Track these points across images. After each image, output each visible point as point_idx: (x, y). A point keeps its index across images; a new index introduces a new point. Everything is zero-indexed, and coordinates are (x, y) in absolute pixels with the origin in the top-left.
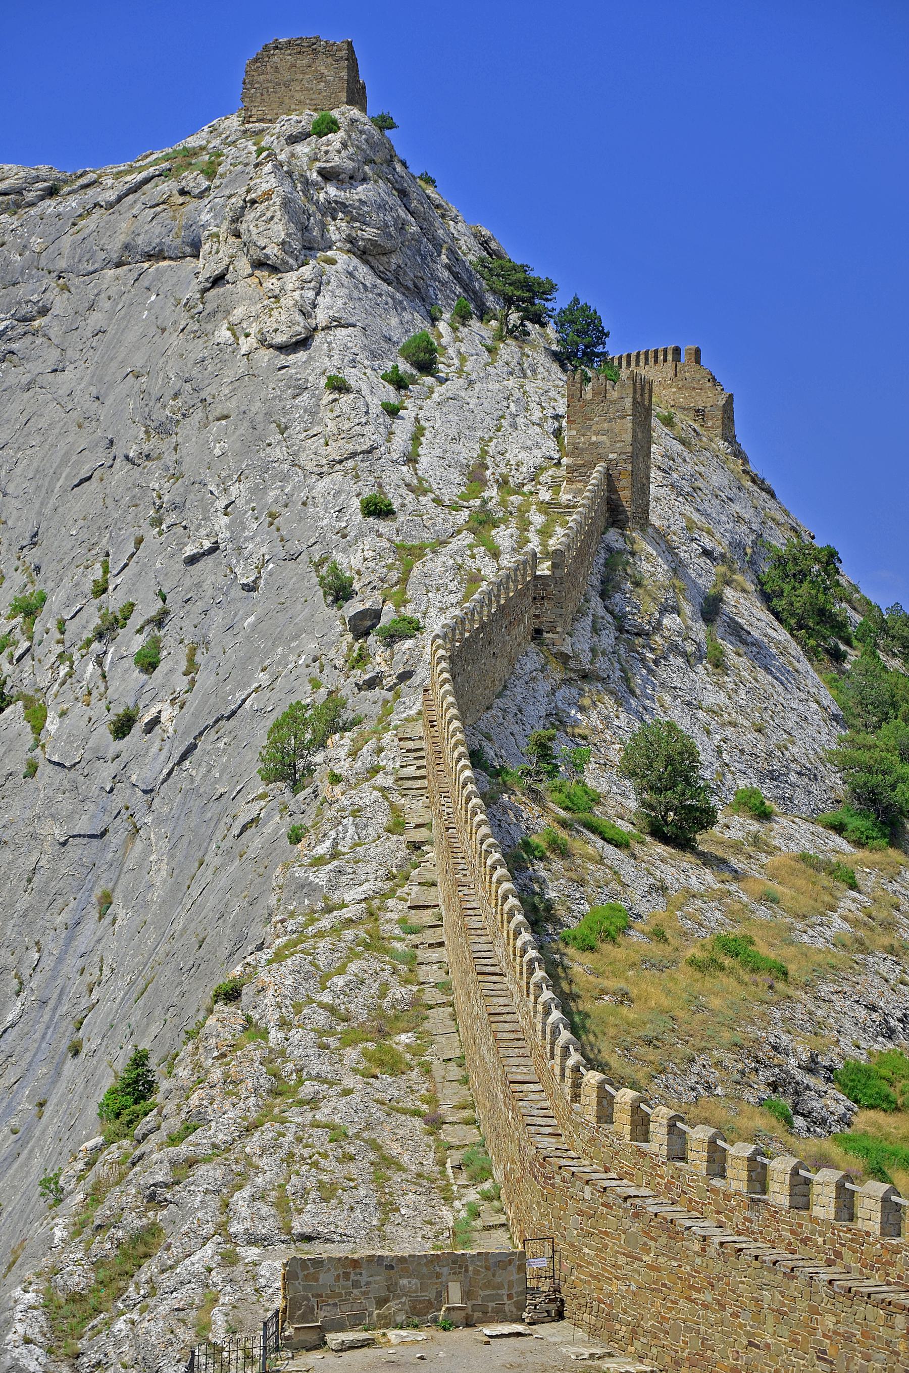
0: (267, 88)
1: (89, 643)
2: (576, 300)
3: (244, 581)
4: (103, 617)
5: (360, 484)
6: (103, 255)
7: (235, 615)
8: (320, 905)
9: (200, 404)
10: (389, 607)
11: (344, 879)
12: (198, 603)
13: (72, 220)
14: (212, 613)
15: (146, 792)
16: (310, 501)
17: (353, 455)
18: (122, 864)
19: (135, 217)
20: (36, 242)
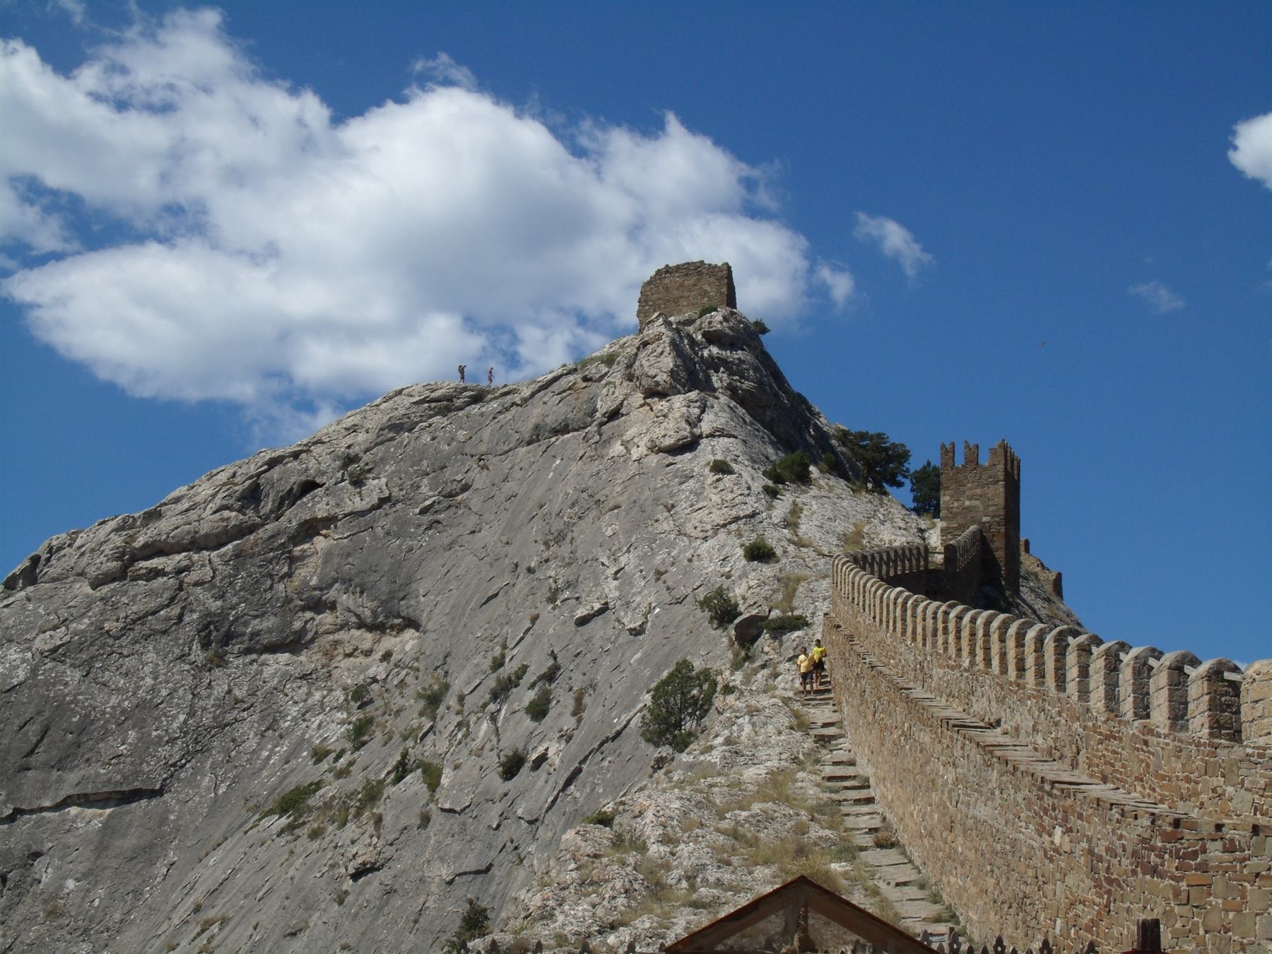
0: (659, 305)
1: (485, 705)
2: (929, 464)
3: (632, 626)
5: (743, 539)
6: (517, 436)
7: (623, 655)
9: (594, 506)
12: (587, 656)
13: (492, 416)
14: (600, 661)
15: (530, 822)
16: (695, 558)
17: (737, 519)
18: (504, 895)
19: (545, 403)
20: (462, 435)
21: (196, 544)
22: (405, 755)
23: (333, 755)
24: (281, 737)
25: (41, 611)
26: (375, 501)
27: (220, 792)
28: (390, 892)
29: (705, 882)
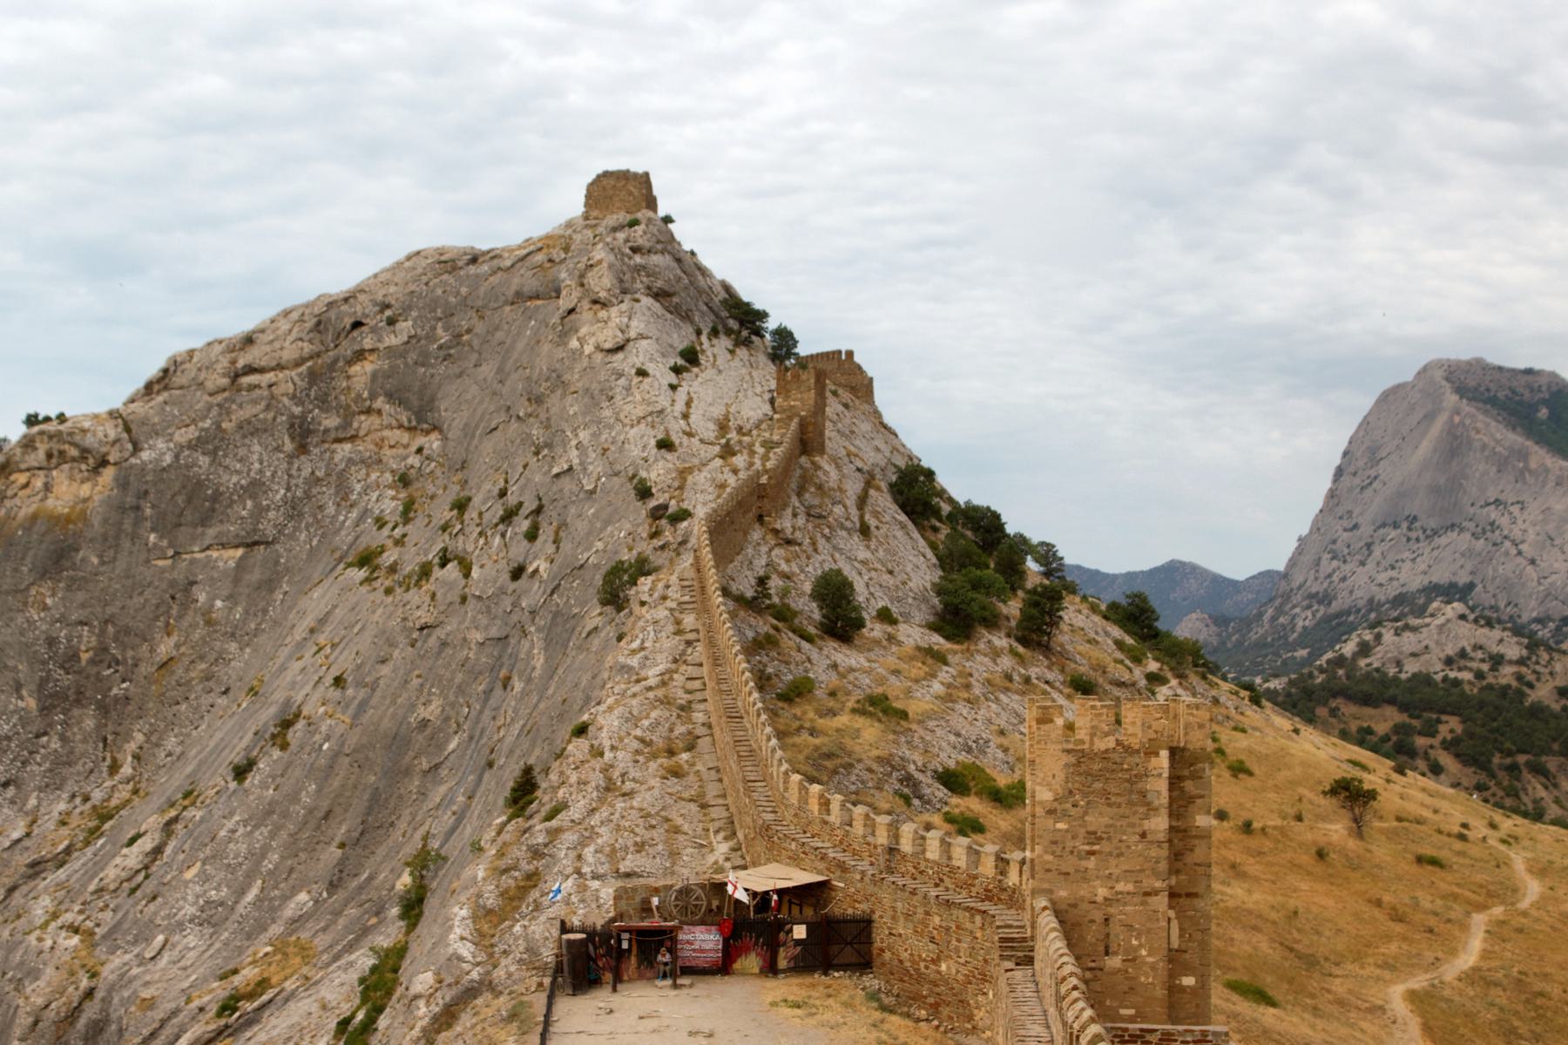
1: (497, 525)
4: (505, 510)
8: (634, 678)
10: (673, 502)
11: (648, 663)
17: (651, 413)
20: (464, 290)
21: (280, 367)
22: (445, 550)
23: (390, 525)
24: (351, 506)
25: (176, 412)
26: (406, 339)
27: (315, 543)
28: (444, 644)
29: (629, 780)
